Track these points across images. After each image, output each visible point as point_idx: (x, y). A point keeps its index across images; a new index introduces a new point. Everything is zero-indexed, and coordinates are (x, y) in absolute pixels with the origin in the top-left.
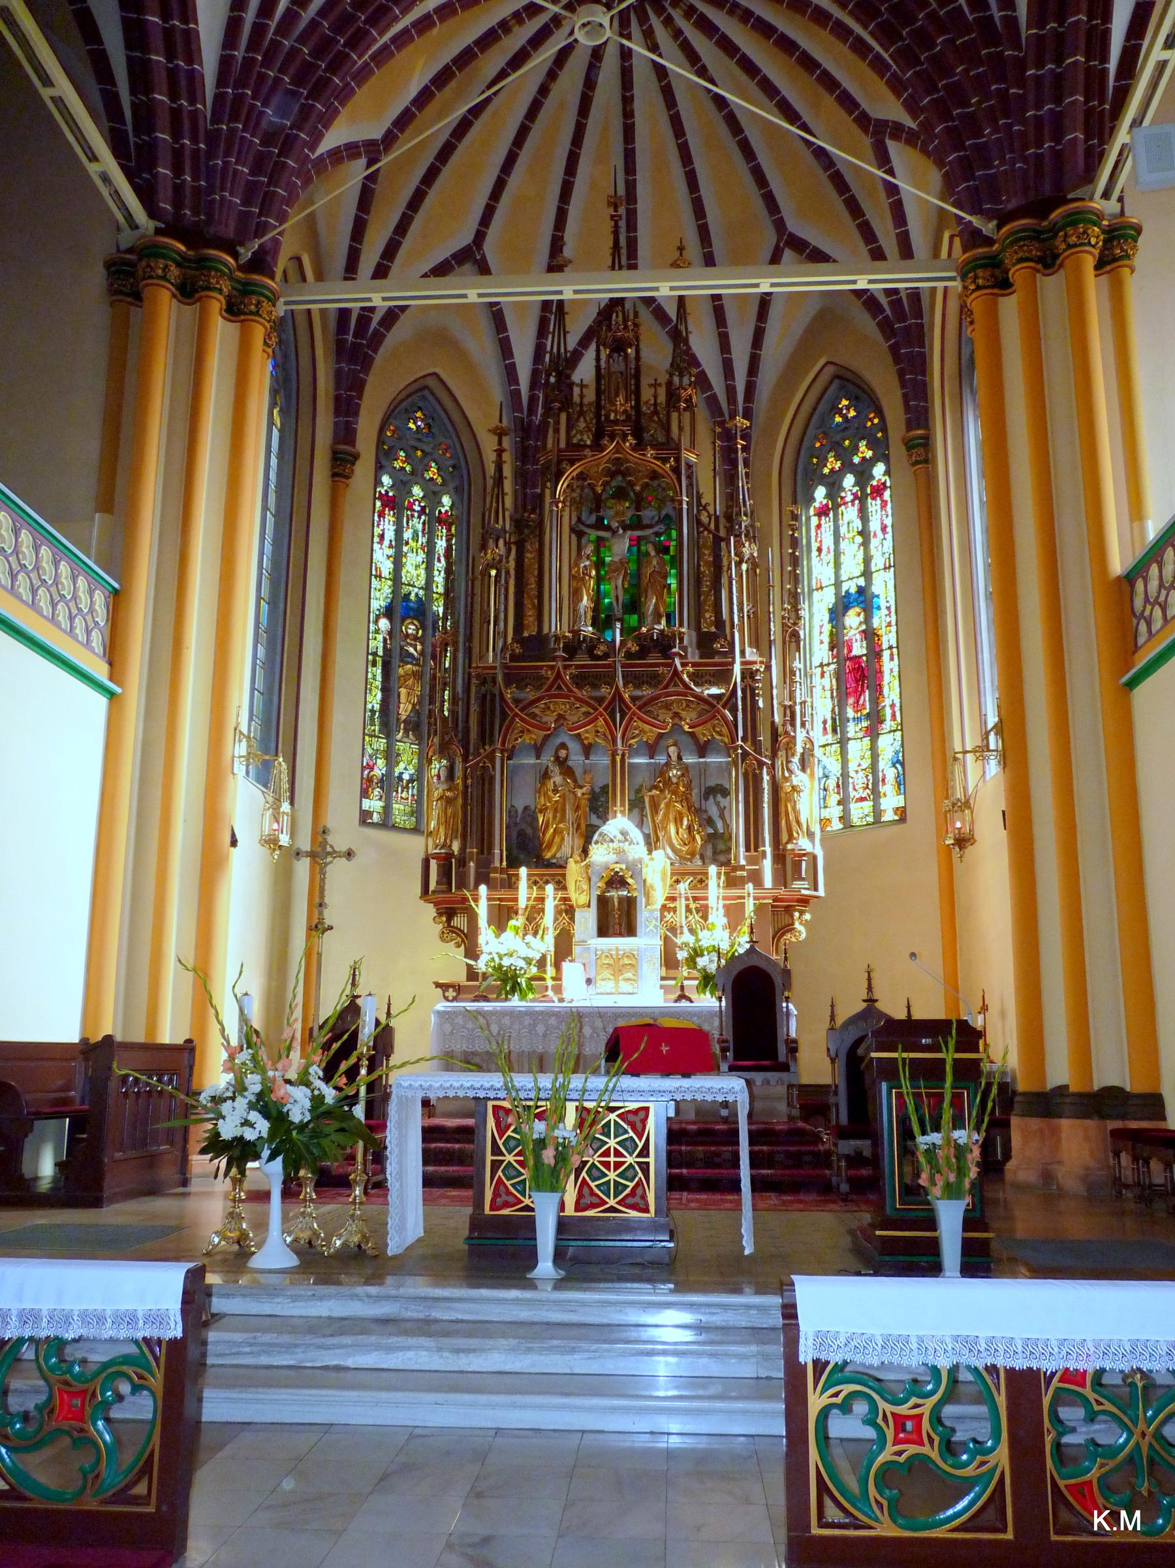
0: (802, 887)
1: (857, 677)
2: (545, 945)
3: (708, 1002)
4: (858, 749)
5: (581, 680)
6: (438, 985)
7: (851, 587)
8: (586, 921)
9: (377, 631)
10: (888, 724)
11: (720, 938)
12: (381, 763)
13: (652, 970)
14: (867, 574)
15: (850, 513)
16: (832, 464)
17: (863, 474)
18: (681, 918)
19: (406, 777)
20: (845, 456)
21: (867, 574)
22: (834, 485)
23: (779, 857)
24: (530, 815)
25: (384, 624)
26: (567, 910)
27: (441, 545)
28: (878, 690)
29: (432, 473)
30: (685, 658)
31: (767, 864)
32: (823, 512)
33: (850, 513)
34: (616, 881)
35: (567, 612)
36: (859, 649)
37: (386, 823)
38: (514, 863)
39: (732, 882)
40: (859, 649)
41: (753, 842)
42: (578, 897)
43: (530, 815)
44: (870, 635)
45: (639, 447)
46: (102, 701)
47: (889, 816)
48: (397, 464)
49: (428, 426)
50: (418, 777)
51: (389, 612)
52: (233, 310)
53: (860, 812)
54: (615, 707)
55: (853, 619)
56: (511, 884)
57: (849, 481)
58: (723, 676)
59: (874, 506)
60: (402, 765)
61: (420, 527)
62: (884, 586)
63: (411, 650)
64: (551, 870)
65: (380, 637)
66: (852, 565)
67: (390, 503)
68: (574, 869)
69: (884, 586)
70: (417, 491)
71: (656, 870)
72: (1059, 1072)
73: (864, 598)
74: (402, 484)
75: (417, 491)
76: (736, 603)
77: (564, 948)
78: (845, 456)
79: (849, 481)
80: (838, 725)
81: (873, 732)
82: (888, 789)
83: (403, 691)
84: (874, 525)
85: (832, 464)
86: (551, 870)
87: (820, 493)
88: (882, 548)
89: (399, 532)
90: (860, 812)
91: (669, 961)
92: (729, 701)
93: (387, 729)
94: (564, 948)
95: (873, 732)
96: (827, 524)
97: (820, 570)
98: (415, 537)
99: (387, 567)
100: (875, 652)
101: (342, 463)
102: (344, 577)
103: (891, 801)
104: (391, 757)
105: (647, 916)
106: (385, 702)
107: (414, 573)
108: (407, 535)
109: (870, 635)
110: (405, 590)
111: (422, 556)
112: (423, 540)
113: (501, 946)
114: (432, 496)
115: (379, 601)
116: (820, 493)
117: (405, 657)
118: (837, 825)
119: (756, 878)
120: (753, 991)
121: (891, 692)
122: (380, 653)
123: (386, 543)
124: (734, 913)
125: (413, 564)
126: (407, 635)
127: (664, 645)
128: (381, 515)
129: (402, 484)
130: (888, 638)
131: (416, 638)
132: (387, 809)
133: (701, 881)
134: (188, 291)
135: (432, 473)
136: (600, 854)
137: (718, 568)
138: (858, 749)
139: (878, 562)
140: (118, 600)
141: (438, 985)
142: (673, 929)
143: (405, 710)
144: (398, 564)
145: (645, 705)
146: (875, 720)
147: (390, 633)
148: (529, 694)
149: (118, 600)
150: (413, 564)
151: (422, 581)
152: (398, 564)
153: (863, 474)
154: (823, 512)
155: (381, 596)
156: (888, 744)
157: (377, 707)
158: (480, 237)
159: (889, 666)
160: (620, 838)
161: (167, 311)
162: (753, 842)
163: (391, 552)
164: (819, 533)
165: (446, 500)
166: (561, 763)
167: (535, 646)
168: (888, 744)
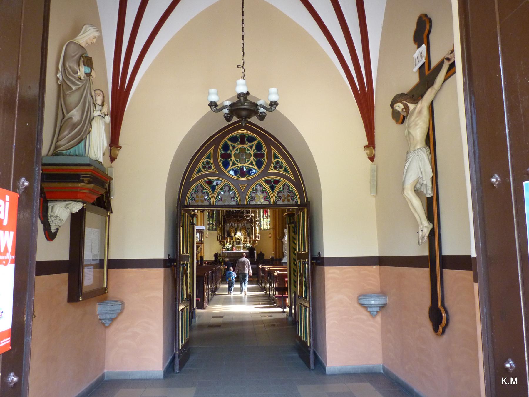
0: (257, 239)
2: (231, 246)
4: (265, 220)
8: (235, 243)
23: (255, 236)
24: (229, 231)
26: (233, 242)
34: (238, 239)
38: (228, 237)
41: (252, 234)
43: (229, 231)
53: (265, 228)
56: (227, 239)
64: (232, 238)
80: (263, 217)
81: (267, 218)
86: (232, 238)
90: (265, 228)
92: (250, 219)
94: (233, 246)
104: (209, 221)
113: (228, 246)
121: (269, 214)
124: (250, 242)
136: (236, 236)
138: (265, 220)
143: (210, 215)
146: (267, 217)
156: (269, 220)
160: (239, 234)
162: (252, 234)
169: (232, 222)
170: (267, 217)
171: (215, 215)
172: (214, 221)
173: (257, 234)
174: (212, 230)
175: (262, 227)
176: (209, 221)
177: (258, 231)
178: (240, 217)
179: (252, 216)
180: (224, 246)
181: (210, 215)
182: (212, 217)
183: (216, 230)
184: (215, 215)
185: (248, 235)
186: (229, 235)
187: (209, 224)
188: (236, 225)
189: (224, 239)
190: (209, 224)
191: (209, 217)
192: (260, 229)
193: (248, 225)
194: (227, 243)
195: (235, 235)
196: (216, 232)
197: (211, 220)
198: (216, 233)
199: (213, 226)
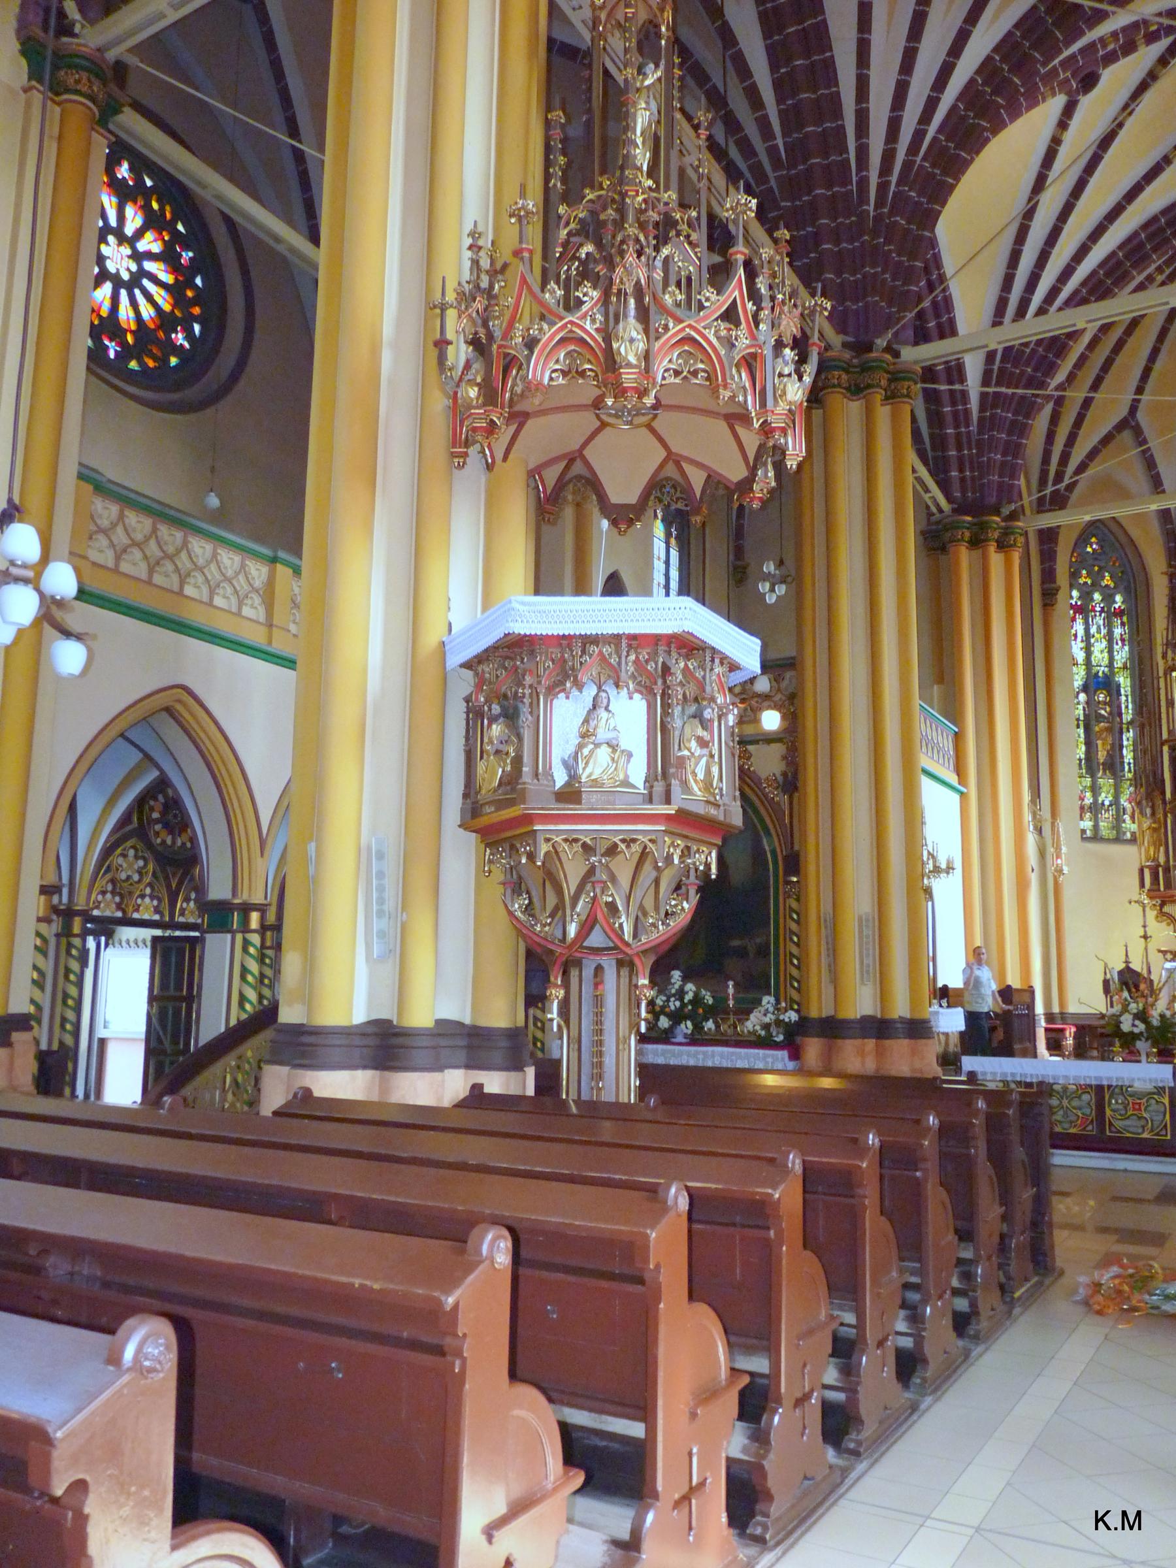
6: (1160, 951)
9: (1078, 703)
12: (1088, 794)
19: (1107, 803)
25: (1082, 697)
27: (1118, 631)
29: (1107, 580)
37: (1096, 837)
46: (957, 797)
48: (1081, 581)
49: (1102, 547)
51: (1085, 688)
52: (1002, 546)
60: (1103, 795)
61: (1101, 622)
63: (1103, 712)
65: (1081, 707)
67: (1078, 609)
70: (1097, 596)
74: (1086, 595)
75: (1097, 596)
83: (1099, 742)
89: (1087, 630)
98: (1099, 631)
99: (1080, 656)
101: (1049, 596)
102: (1057, 673)
104: (1095, 790)
106: (1088, 752)
107: (1100, 656)
108: (1093, 630)
110: (1095, 670)
111: (1105, 643)
112: (1104, 631)
114: (1108, 598)
115: (1078, 683)
122: (1082, 718)
123: (1079, 639)
126: (1099, 702)
128: (1074, 619)
129: (1086, 595)
131: (1105, 703)
132: (1096, 827)
134: (976, 543)
135: (1107, 580)
140: (958, 738)
141: (1160, 951)
143: (1102, 756)
147: (1087, 703)
149: (958, 738)
151: (1106, 662)
155: (1079, 677)
157: (1083, 756)
158: (1133, 409)
161: (964, 556)
163: (1083, 645)
165: (1118, 598)
171: (1128, 756)
172: (1127, 791)
174: (1118, 840)
176: (1095, 790)
181: (1102, 756)
182: (1113, 765)
183: (1133, 840)
184: (1128, 756)
187: (1095, 809)
190: (1095, 809)
191: (1090, 764)
196: (1132, 850)
197: (1106, 783)
198: (1131, 858)
199: (1118, 820)
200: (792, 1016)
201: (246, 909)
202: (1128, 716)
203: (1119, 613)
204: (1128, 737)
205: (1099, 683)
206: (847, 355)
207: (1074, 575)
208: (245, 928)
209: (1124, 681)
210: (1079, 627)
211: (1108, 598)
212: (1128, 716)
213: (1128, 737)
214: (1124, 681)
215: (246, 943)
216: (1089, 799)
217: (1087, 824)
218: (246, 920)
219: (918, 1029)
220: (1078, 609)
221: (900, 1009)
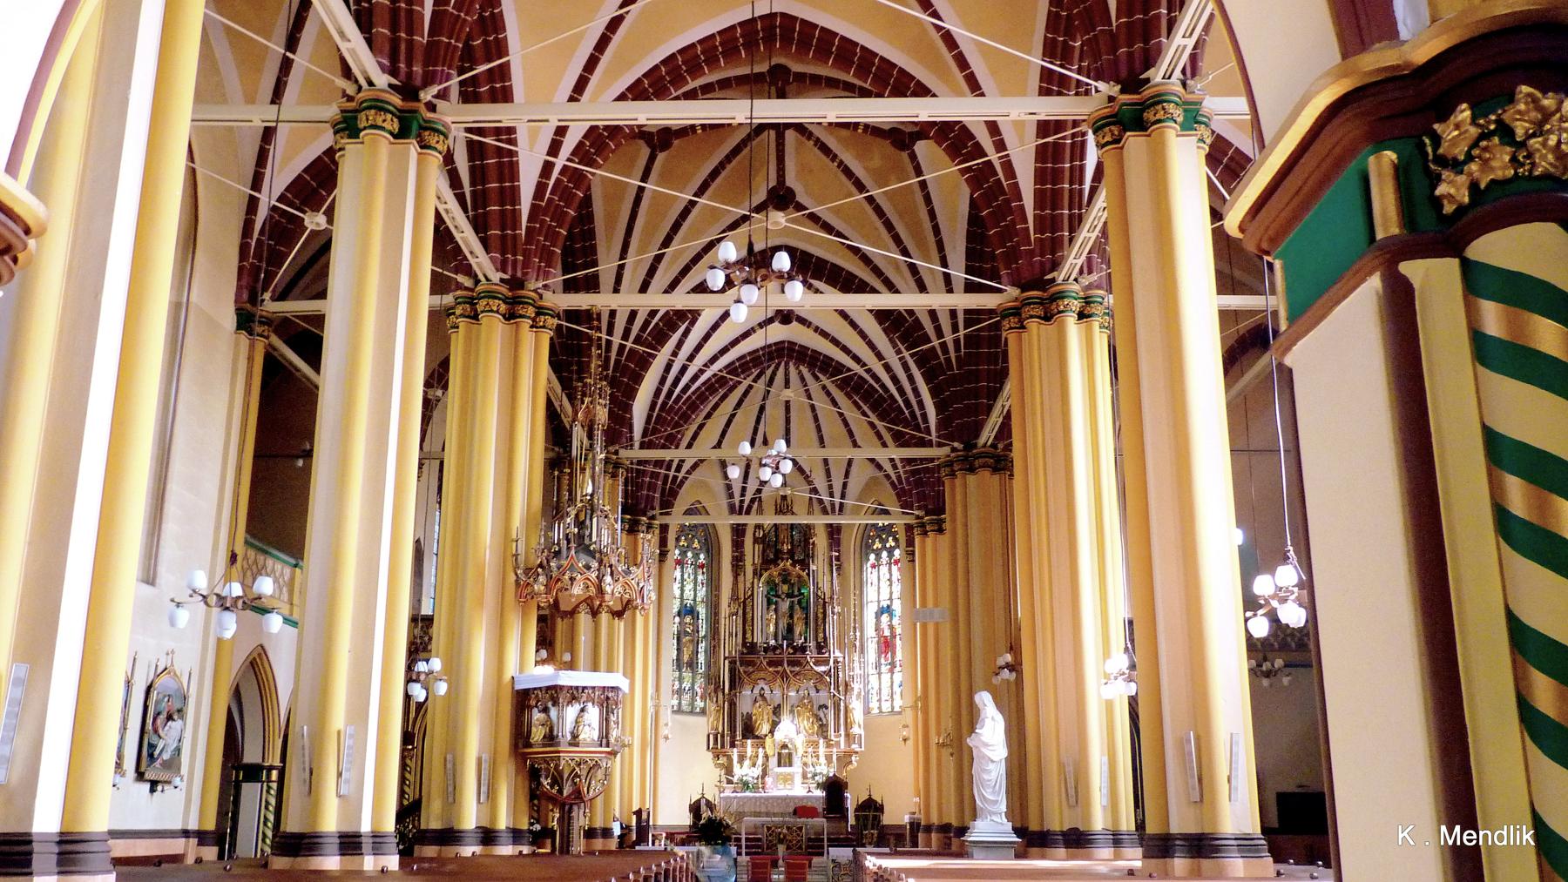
0: (855, 747)
1: (886, 645)
2: (757, 771)
3: (820, 793)
4: (886, 677)
5: (771, 664)
7: (885, 604)
8: (773, 761)
10: (898, 668)
11: (825, 770)
13: (798, 779)
14: (891, 599)
15: (884, 569)
16: (878, 545)
17: (891, 555)
18: (809, 760)
20: (884, 542)
21: (891, 599)
22: (878, 554)
23: (847, 735)
24: (749, 716)
26: (766, 757)
27: (700, 578)
28: (894, 653)
29: (696, 545)
30: (811, 655)
31: (842, 739)
32: (873, 566)
33: (884, 569)
34: (785, 746)
35: (766, 629)
36: (887, 633)
38: (745, 737)
39: (829, 746)
40: (887, 633)
41: (837, 730)
42: (770, 752)
44: (891, 627)
45: (793, 565)
47: (897, 709)
50: (692, 688)
51: (679, 614)
53: (886, 707)
54: (784, 676)
55: (885, 618)
57: (884, 554)
58: (826, 662)
59: (895, 568)
62: (897, 606)
64: (760, 740)
66: (885, 595)
67: (679, 562)
68: (768, 740)
69: (897, 606)
71: (800, 742)
72: (935, 820)
73: (888, 610)
74: (683, 553)
75: (690, 554)
76: (832, 629)
77: (765, 773)
78: (884, 542)
79: (884, 554)
80: (878, 666)
81: (891, 671)
82: (897, 697)
84: (894, 578)
85: (878, 545)
86: (760, 740)
87: (872, 557)
88: (897, 588)
91: (804, 776)
92: (828, 673)
93: (679, 668)
94: (765, 773)
95: (891, 671)
96: (875, 571)
97: (871, 593)
99: (677, 593)
100: (893, 636)
101: (663, 555)
103: (898, 703)
104: (681, 679)
105: (797, 761)
109: (891, 627)
113: (744, 771)
114: (696, 556)
115: (676, 610)
116: (872, 557)
117: (686, 634)
118: (876, 711)
119: (838, 743)
120: (835, 788)
121: (899, 655)
124: (829, 758)
125: (689, 587)
127: (803, 649)
129: (683, 553)
130: (898, 631)
133: (816, 745)
135: (696, 545)
136: (780, 735)
137: (824, 613)
138: (886, 677)
139: (896, 595)
142: (805, 764)
143: (686, 658)
144: (682, 591)
145: (796, 674)
146: (893, 665)
148: (751, 669)
150: (689, 587)
152: (682, 591)
153: (891, 555)
154: (873, 566)
156: (898, 677)
159: (898, 642)
162: (837, 730)
164: (871, 575)
166: (762, 696)
167: (751, 648)
168: (898, 677)
169: (762, 684)
170: (893, 665)
171: (701, 658)
172: (700, 682)
173: (856, 730)
174: (692, 712)
175: (874, 705)
176: (681, 679)
177: (858, 714)
178: (792, 663)
179: (836, 662)
180: (729, 771)
181: (686, 658)
182: (692, 665)
183: (703, 712)
184: (701, 658)
185: (823, 729)
186: (749, 731)
187: (680, 692)
188: (777, 693)
189: (733, 745)
190: (680, 692)
192: (867, 711)
193: (823, 694)
194: (742, 758)
195: (772, 732)
196: (702, 720)
197: (687, 675)
198: (702, 726)
199: (693, 699)
200: (538, 827)
201: (271, 768)
202: (702, 633)
203: (702, 566)
204: (702, 646)
205: (688, 611)
206: (504, 290)
207: (678, 540)
208: (269, 780)
209: (702, 610)
210: (678, 574)
211: (696, 556)
212: (702, 633)
213: (702, 646)
214: (702, 610)
215: (269, 788)
216: (677, 686)
217: (675, 702)
218: (269, 776)
219: (607, 833)
220: (679, 562)
221: (598, 824)
